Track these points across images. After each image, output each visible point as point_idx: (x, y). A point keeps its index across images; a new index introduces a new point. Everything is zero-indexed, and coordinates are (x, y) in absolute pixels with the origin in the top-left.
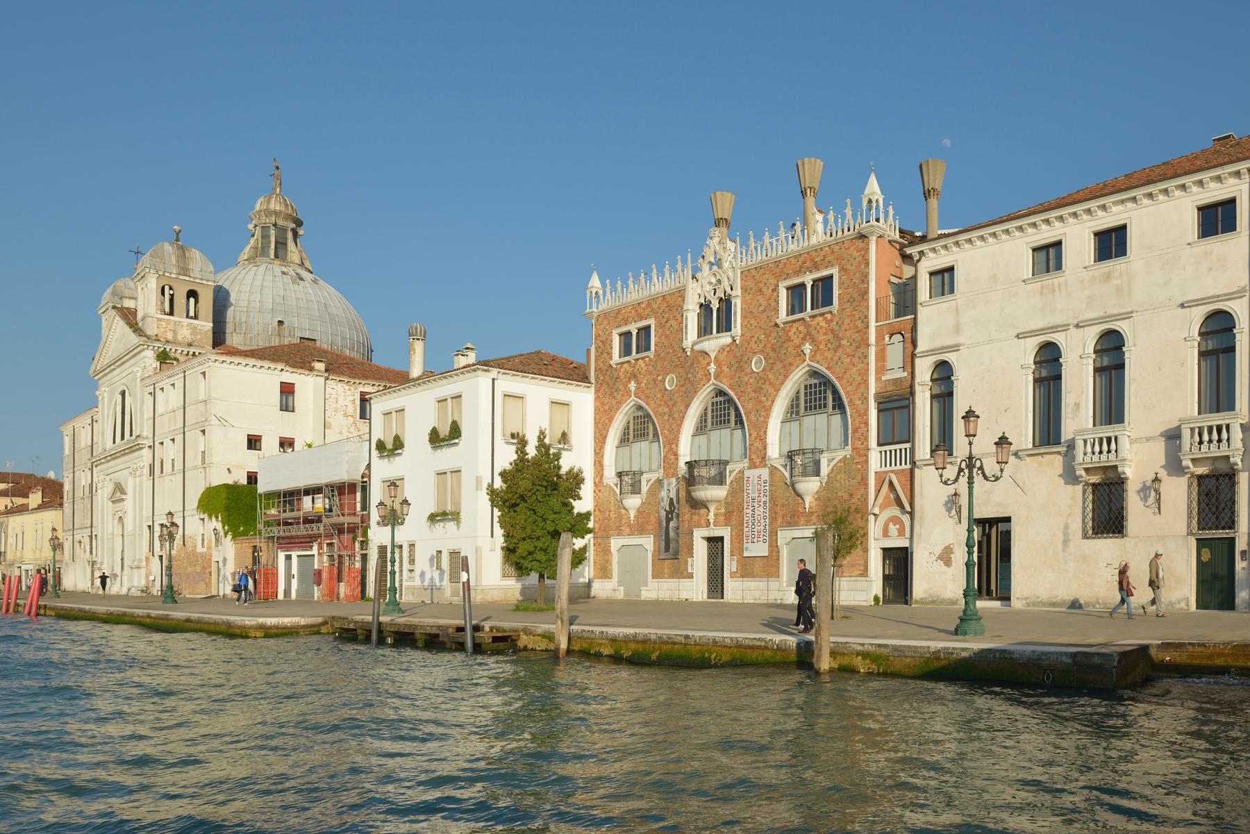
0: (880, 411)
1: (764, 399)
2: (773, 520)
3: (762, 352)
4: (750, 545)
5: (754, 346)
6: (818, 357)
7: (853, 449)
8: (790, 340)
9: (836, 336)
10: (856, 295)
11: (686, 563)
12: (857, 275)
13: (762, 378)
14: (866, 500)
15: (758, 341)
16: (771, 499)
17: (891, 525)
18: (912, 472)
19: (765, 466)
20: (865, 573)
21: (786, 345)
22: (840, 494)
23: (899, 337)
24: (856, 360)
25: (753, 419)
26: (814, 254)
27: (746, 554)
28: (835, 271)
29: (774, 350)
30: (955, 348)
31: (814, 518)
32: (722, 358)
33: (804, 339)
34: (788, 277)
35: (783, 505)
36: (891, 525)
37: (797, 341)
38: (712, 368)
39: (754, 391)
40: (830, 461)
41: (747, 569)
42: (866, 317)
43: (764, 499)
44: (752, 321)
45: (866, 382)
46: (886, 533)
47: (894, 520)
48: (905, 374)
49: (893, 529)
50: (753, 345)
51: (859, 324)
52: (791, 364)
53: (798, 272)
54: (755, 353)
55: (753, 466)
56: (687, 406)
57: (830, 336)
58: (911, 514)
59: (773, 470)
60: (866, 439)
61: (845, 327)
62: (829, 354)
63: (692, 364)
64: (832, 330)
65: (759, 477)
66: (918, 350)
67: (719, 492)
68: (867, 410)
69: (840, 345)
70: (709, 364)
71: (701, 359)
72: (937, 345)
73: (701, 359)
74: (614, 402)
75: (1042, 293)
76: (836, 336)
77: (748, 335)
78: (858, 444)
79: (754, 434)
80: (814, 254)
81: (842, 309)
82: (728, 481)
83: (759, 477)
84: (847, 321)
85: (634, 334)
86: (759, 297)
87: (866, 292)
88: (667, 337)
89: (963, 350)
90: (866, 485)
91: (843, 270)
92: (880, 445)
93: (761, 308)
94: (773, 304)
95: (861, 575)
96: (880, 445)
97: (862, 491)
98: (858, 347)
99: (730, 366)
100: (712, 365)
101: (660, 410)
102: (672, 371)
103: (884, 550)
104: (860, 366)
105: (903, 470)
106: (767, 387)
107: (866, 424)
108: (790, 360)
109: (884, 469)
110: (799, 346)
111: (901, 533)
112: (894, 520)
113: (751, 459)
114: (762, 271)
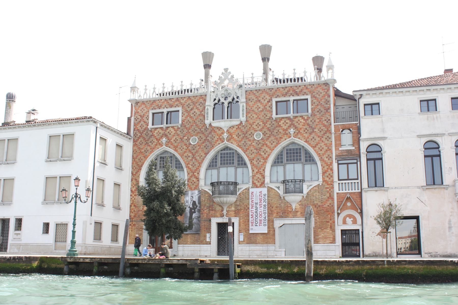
0: (338, 164)
1: (263, 154)
2: (270, 213)
3: (261, 130)
4: (254, 227)
5: (255, 127)
6: (299, 136)
7: (324, 181)
8: (280, 126)
9: (310, 127)
10: (322, 109)
11: (205, 236)
12: (323, 100)
13: (262, 143)
14: (333, 206)
15: (258, 125)
16: (268, 203)
17: (348, 218)
18: (361, 193)
19: (264, 187)
20: (334, 241)
21: (278, 129)
22: (316, 202)
23: (349, 131)
24: (324, 139)
25: (255, 163)
26: (295, 88)
27: (251, 232)
28: (309, 97)
29: (268, 129)
30: (384, 138)
31: (299, 213)
32: (232, 131)
33: (289, 127)
34: (278, 96)
35: (277, 207)
36: (348, 218)
37: (285, 128)
38: (225, 135)
39: (256, 149)
40: (309, 186)
41: (251, 239)
42: (329, 120)
43: (265, 203)
44: (254, 115)
45: (330, 149)
46: (344, 222)
47: (350, 216)
48: (354, 148)
49: (349, 220)
50: (254, 126)
51: (325, 123)
52: (281, 138)
53: (284, 95)
54: (256, 131)
55: (255, 185)
56: (206, 154)
57: (306, 127)
58: (361, 213)
59: (270, 189)
60: (332, 176)
61: (316, 123)
62: (306, 135)
63: (210, 133)
64: (308, 124)
65: (261, 192)
66: (361, 138)
67: (232, 199)
68: (331, 163)
69: (313, 131)
70: (223, 133)
71: (217, 130)
72: (372, 136)
73: (217, 130)
74: (149, 148)
75: (428, 119)
76: (310, 127)
77: (251, 121)
78: (327, 179)
79: (256, 171)
80: (295, 88)
81: (313, 115)
82: (238, 193)
83: (261, 192)
84: (317, 121)
85: (165, 114)
86: (259, 104)
87: (329, 108)
88: (191, 117)
89: (387, 141)
90: (333, 199)
91: (313, 97)
92: (339, 180)
93: (260, 110)
94: (268, 108)
95: (331, 243)
96: (339, 180)
97: (330, 201)
98: (324, 134)
99: (238, 136)
100: (225, 134)
101: (186, 154)
102: (196, 135)
103: (342, 230)
104: (326, 142)
105: (355, 193)
106: (265, 147)
107: (332, 170)
108: (280, 136)
109: (341, 191)
110: (287, 130)
111: (355, 222)
112: (350, 216)
113: (253, 183)
114: (260, 92)
